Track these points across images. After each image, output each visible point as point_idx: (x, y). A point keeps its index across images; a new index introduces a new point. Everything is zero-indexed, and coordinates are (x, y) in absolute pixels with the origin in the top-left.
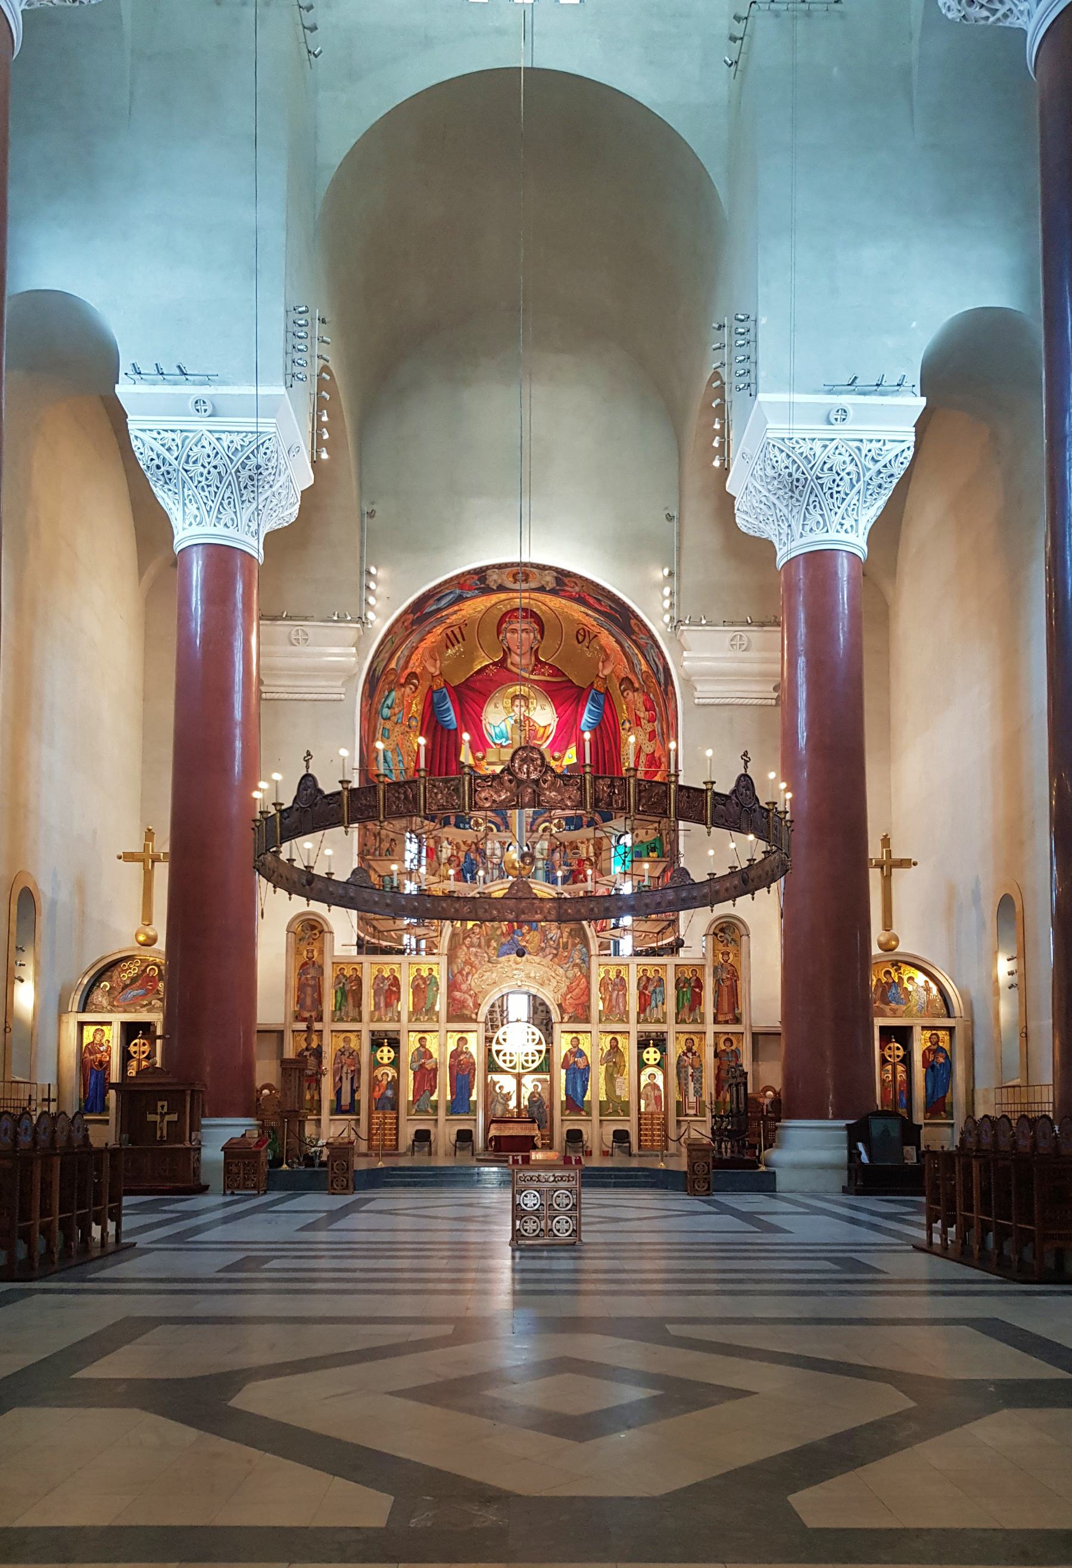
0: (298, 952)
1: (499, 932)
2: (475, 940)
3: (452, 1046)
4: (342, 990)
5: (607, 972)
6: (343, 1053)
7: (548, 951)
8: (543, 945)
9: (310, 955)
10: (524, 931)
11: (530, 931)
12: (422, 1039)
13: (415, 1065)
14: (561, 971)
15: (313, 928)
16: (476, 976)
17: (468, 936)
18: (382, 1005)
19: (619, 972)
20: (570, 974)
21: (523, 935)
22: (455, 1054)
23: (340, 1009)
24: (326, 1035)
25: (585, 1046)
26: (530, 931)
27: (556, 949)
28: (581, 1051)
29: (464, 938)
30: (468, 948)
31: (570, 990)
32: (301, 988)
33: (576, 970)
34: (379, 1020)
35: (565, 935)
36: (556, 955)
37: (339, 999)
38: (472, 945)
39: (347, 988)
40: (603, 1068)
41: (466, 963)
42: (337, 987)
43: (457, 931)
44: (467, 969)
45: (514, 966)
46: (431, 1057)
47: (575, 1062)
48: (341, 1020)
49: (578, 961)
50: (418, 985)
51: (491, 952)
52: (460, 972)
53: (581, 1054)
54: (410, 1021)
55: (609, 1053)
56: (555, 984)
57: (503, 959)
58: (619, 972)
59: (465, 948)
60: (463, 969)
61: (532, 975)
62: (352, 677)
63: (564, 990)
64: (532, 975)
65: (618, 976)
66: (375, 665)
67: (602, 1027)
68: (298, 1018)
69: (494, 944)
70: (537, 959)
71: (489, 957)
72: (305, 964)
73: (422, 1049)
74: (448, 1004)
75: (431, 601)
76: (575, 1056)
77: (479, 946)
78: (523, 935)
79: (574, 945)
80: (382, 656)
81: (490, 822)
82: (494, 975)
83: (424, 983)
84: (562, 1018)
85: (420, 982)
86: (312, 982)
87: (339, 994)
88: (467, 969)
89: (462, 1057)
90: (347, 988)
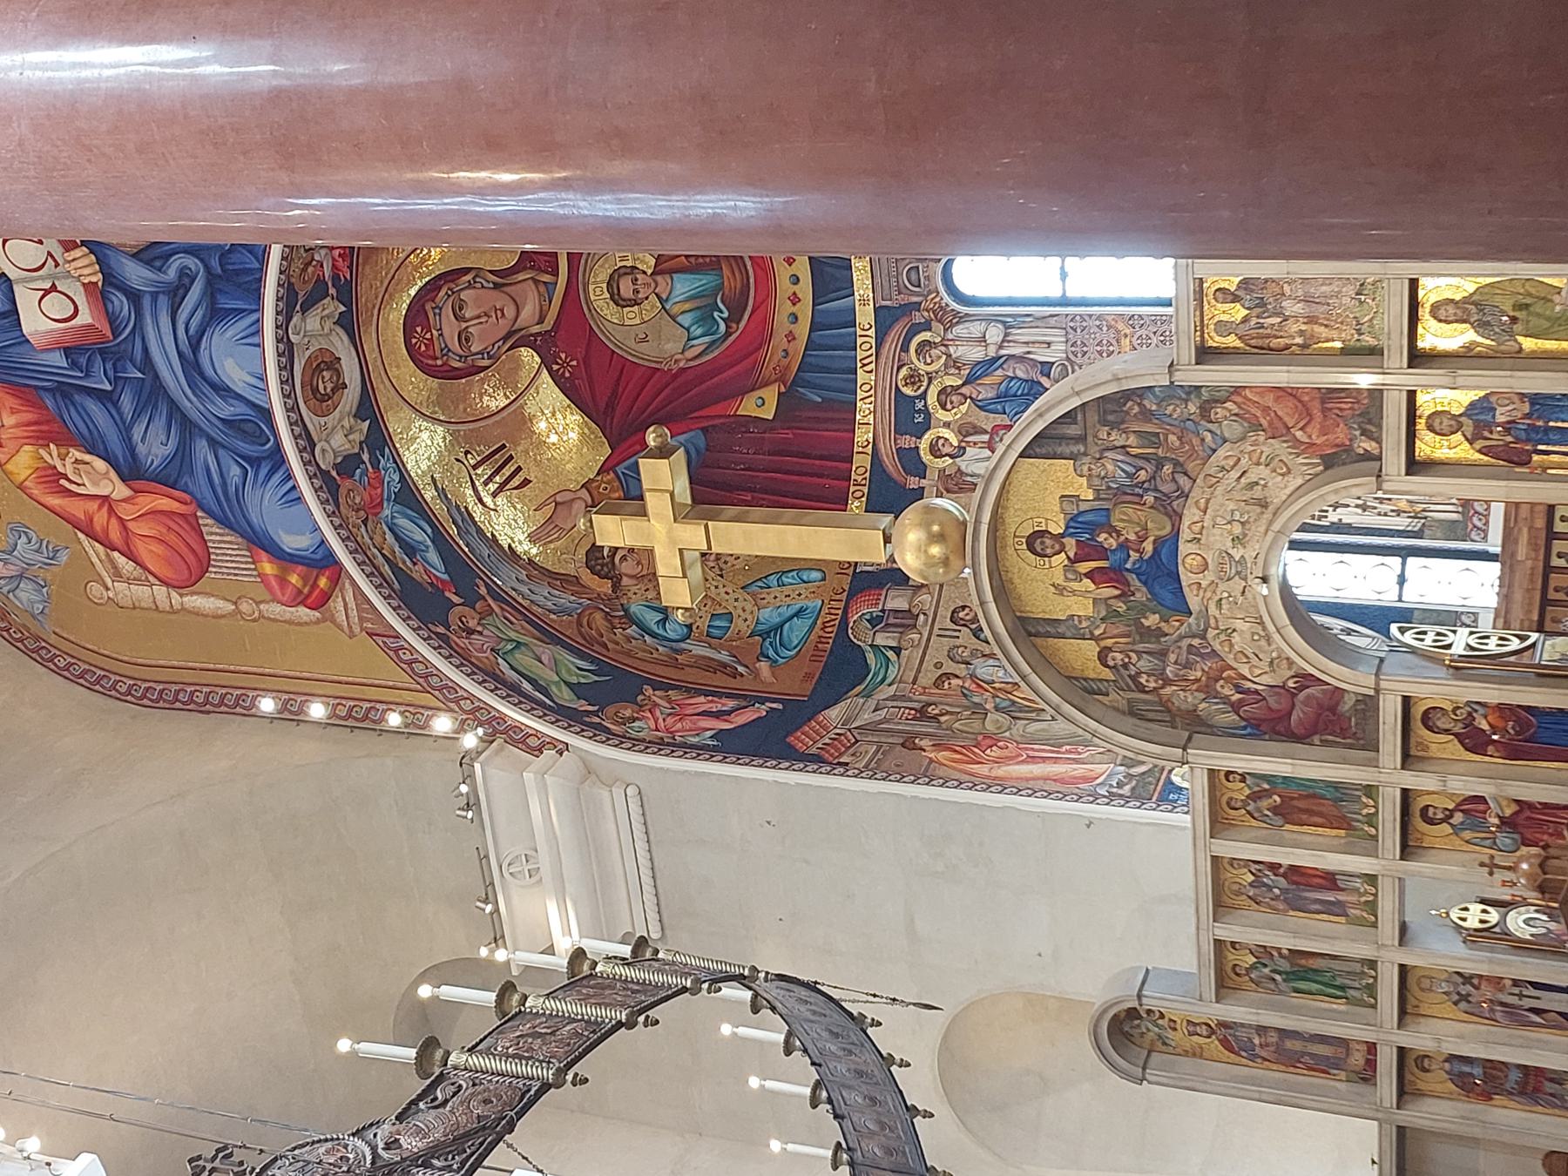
0: (1197, 1053)
1: (1121, 607)
2: (1144, 664)
3: (1444, 746)
4: (1290, 976)
5: (1223, 328)
6: (1465, 998)
7: (1165, 488)
8: (1149, 498)
9: (1204, 1030)
10: (1112, 543)
11: (1113, 531)
12: (1431, 822)
13: (1504, 840)
14: (1221, 453)
15: (1132, 1013)
16: (1245, 671)
17: (1134, 678)
18: (1330, 897)
19: (1224, 295)
20: (1231, 429)
21: (1124, 546)
22: (1474, 741)
23: (1342, 988)
24: (1419, 1039)
25: (1445, 396)
26: (1113, 531)
27: (1159, 466)
28: (1472, 405)
29: (1142, 689)
30: (1167, 682)
31: (1279, 431)
32: (1290, 1060)
33: (1220, 412)
34: (1372, 907)
35: (1117, 438)
36: (1177, 464)
37: (1314, 987)
38: (1160, 675)
39: (1285, 965)
40: (1528, 344)
41: (1209, 691)
42: (1283, 986)
43: (1123, 705)
44: (1227, 691)
45: (1209, 576)
46: (1481, 799)
47: (1508, 427)
48: (1371, 990)
49: (1192, 408)
50: (1275, 810)
51: (1174, 627)
52: (1236, 707)
53: (1480, 413)
54: (1369, 844)
55: (1481, 326)
56: (1263, 471)
57: (1194, 602)
58: (1224, 295)
59: (1168, 690)
60: (1226, 700)
61: (1237, 529)
62: (589, 770)
63: (1279, 447)
64: (1237, 529)
65: (1235, 298)
66: (565, 697)
67: (1397, 355)
68: (1367, 1074)
69: (1152, 620)
70: (1190, 515)
71: (1194, 636)
72: (1225, 1043)
73: (1458, 818)
74: (1325, 743)
75: (417, 573)
76: (1489, 426)
77: (1162, 654)
78: (1124, 546)
79: (1147, 415)
80: (547, 675)
81: (905, 348)
82: (1239, 624)
83: (1266, 794)
84: (1367, 457)
85: (1265, 803)
86: (1273, 1038)
87: (1302, 985)
88: (1228, 691)
89: (1485, 726)
90: (1285, 965)
